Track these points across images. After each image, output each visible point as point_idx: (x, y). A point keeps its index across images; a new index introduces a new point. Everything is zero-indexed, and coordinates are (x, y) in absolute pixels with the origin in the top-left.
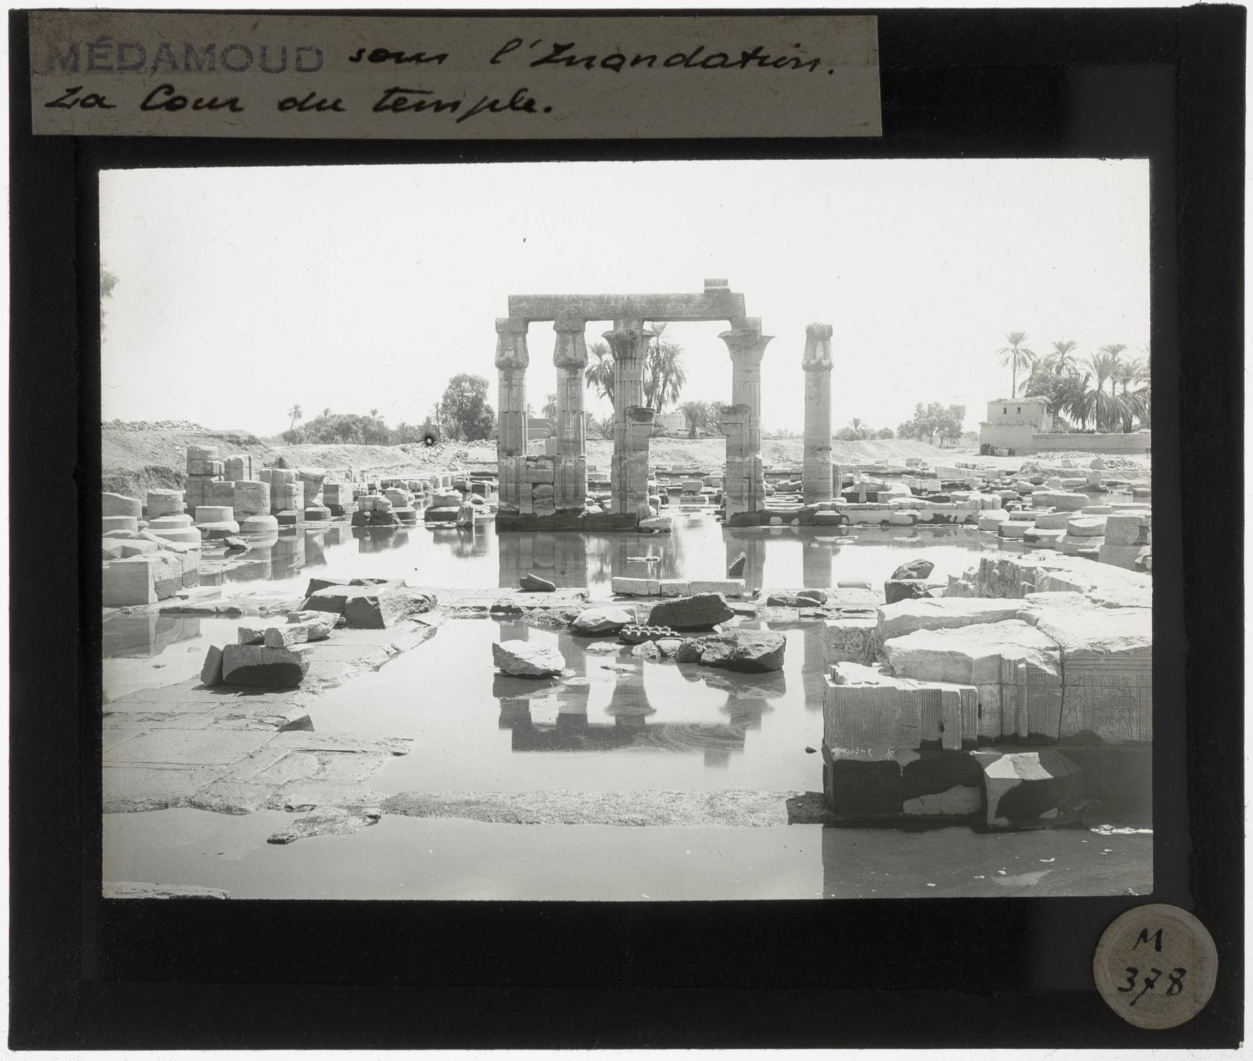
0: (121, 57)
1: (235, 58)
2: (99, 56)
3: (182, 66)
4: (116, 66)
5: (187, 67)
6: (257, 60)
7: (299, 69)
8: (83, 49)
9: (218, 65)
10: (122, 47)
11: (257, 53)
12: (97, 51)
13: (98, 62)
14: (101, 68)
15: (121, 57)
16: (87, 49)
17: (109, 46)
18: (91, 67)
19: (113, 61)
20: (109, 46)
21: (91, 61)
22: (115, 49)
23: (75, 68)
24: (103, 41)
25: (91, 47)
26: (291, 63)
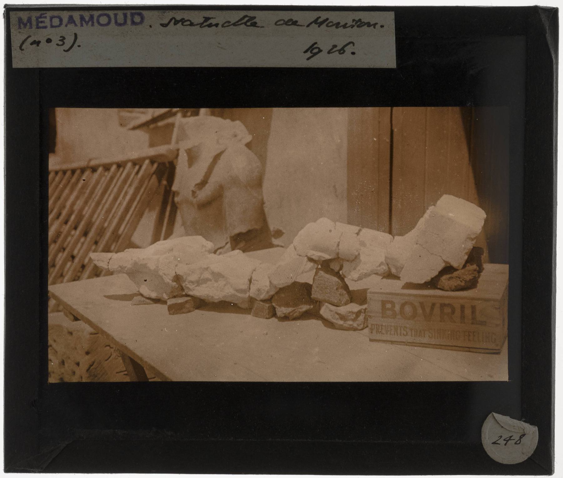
1: (104, 20)
2: (42, 22)
3: (79, 25)
4: (49, 26)
5: (82, 25)
6: (113, 21)
7: (133, 23)
9: (96, 24)
11: (112, 16)
12: (40, 20)
13: (40, 25)
16: (35, 19)
18: (38, 27)
20: (46, 17)
21: (37, 25)
22: (48, 18)
23: (31, 27)
25: (37, 18)
26: (129, 22)
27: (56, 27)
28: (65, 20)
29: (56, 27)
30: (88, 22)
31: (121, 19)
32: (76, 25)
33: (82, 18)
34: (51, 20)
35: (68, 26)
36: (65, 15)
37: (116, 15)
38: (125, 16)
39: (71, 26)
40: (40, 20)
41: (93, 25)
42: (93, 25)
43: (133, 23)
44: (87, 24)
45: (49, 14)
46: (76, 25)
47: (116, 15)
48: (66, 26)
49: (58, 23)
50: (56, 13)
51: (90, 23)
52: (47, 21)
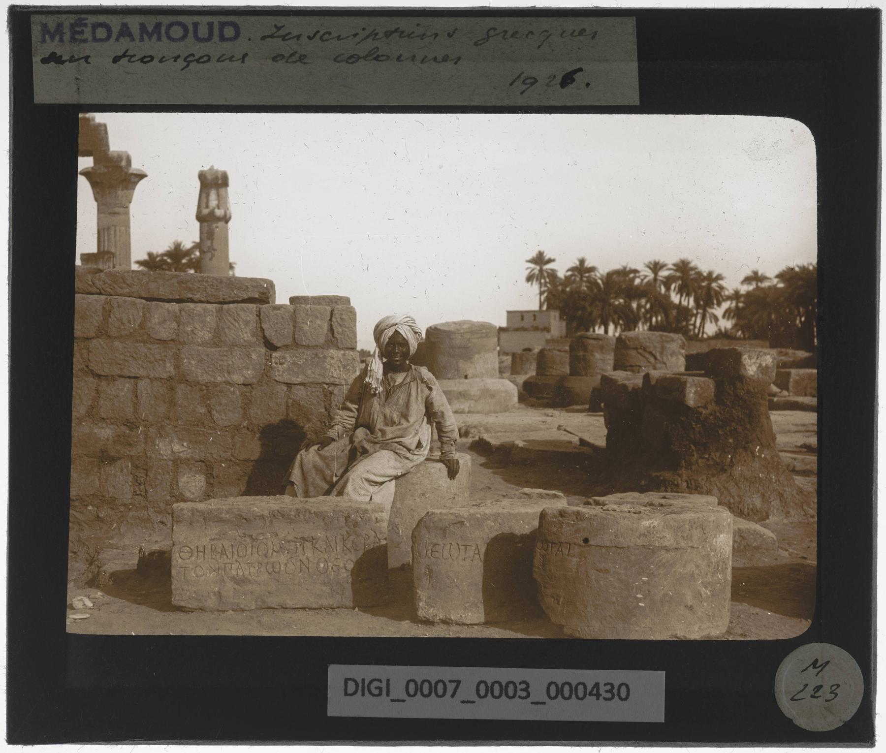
0: (94, 33)
1: (176, 32)
5: (142, 40)
7: (222, 38)
8: (67, 30)
10: (95, 26)
11: (191, 28)
19: (88, 34)
27: (101, 40)
28: (115, 31)
29: (101, 40)
31: (203, 32)
32: (133, 39)
34: (94, 33)
36: (115, 22)
37: (196, 25)
41: (159, 39)
42: (159, 39)
43: (222, 38)
44: (150, 36)
45: (92, 19)
46: (133, 39)
47: (196, 25)
48: (117, 40)
50: (102, 19)
51: (155, 37)
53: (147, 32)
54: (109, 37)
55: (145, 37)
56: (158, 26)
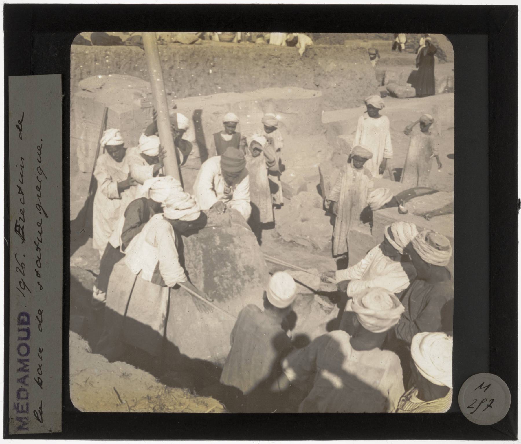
0: (23, 399)
1: (23, 350)
3: (27, 373)
5: (27, 371)
6: (24, 341)
7: (28, 323)
8: (20, 415)
9: (26, 358)
13: (25, 409)
14: (27, 407)
15: (23, 399)
17: (18, 404)
18: (27, 412)
20: (18, 404)
24: (16, 407)
25: (18, 412)
26: (25, 327)
28: (21, 386)
29: (27, 394)
30: (24, 364)
31: (24, 334)
32: (27, 376)
33: (19, 370)
35: (27, 383)
37: (19, 339)
38: (19, 330)
39: (27, 381)
40: (20, 409)
41: (27, 360)
42: (27, 360)
46: (27, 376)
47: (19, 339)
48: (27, 385)
49: (25, 393)
51: (26, 363)
52: (22, 402)
53: (23, 368)
54: (24, 390)
55: (27, 368)
56: (20, 361)
